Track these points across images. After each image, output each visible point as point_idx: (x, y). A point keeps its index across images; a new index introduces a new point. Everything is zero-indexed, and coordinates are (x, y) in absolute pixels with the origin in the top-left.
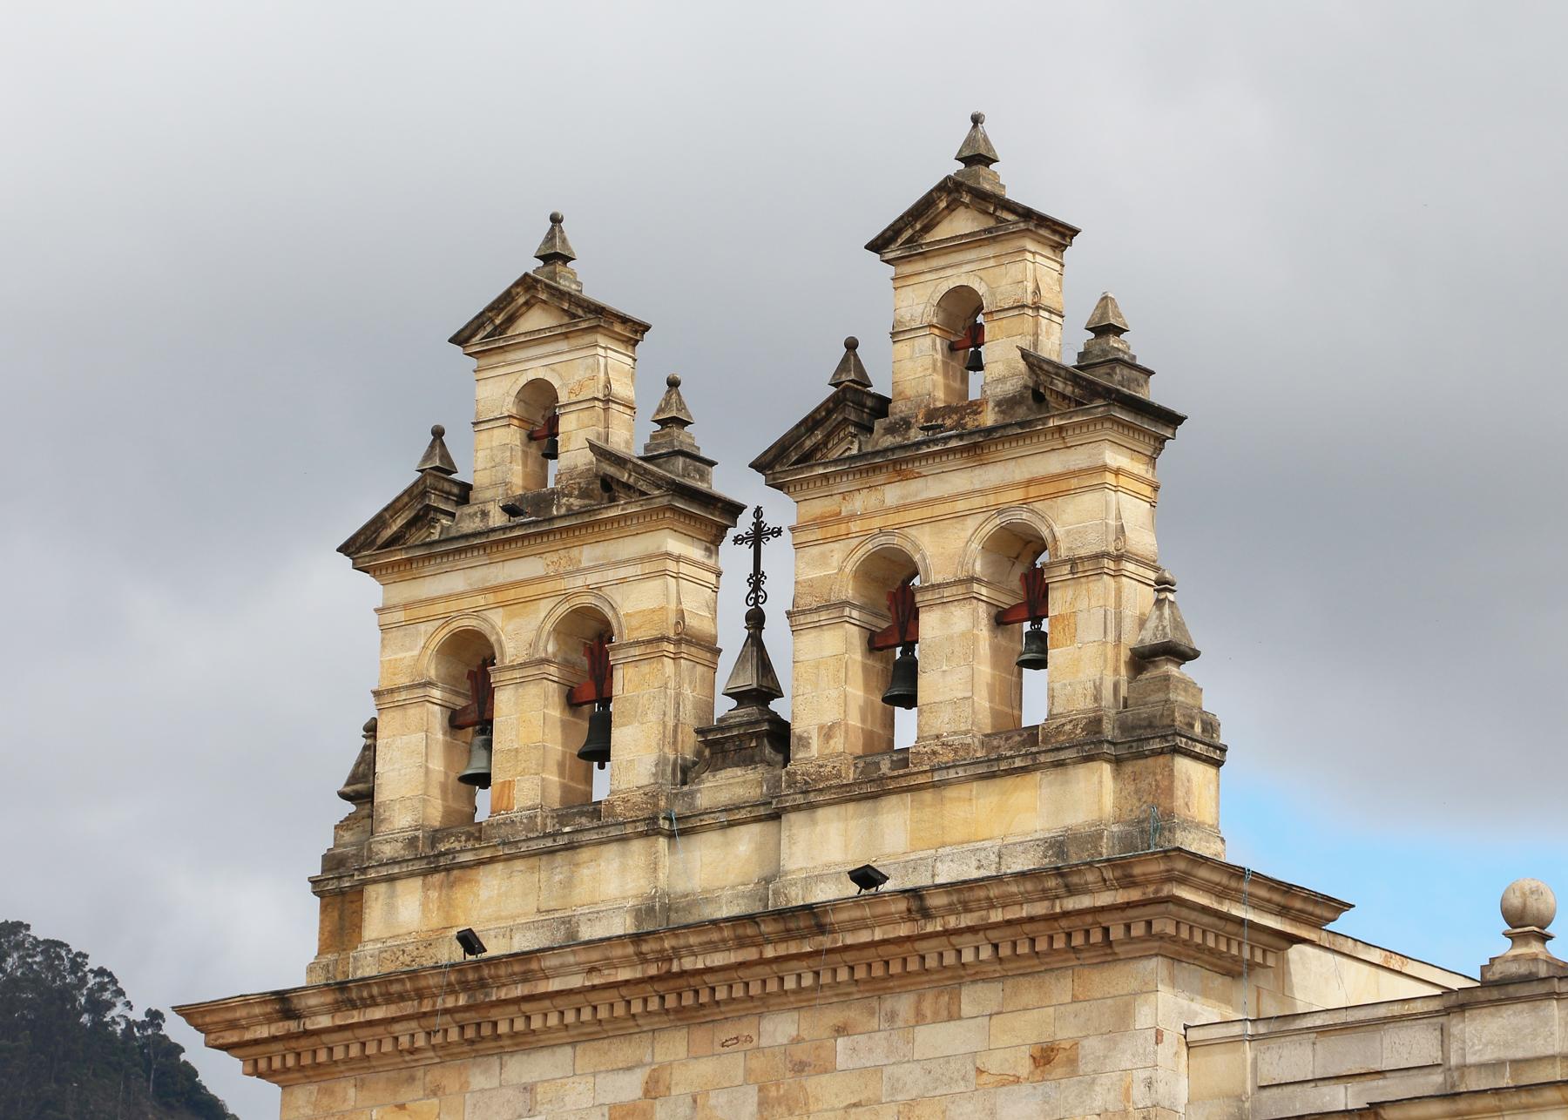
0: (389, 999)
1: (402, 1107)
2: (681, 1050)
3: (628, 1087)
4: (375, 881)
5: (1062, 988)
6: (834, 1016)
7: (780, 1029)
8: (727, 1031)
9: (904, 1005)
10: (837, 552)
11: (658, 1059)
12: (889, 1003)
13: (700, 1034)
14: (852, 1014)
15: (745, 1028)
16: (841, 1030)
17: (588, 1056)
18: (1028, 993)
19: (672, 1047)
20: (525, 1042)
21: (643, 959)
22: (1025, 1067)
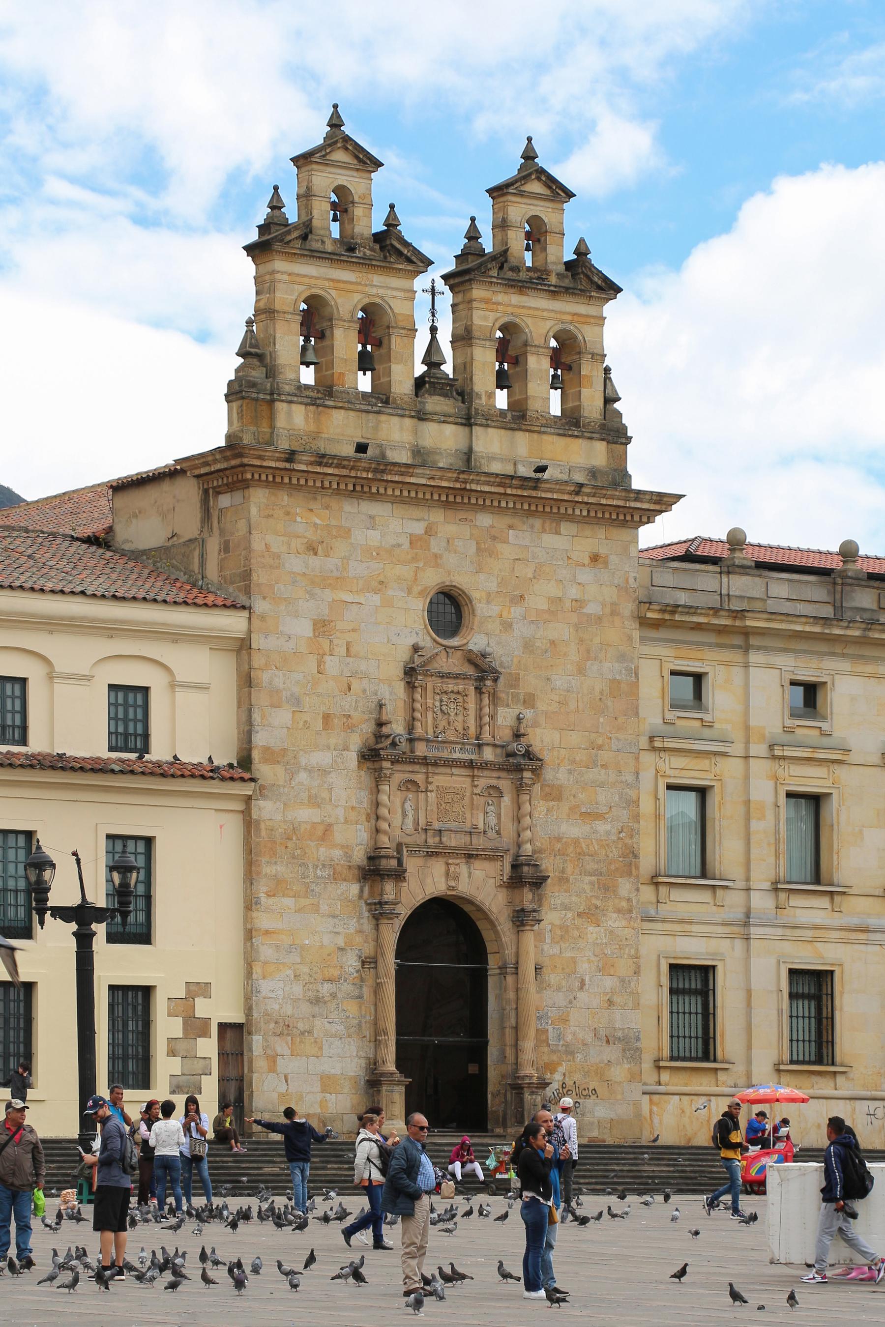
0: (338, 466)
1: (311, 510)
2: (442, 519)
3: (418, 528)
4: (282, 401)
5: (601, 532)
6: (507, 520)
7: (485, 520)
8: (462, 515)
9: (537, 523)
11: (432, 519)
12: (531, 521)
13: (450, 513)
14: (516, 521)
15: (469, 515)
16: (511, 527)
17: (399, 510)
18: (588, 531)
19: (437, 516)
20: (376, 497)
21: (457, 480)
22: (587, 561)
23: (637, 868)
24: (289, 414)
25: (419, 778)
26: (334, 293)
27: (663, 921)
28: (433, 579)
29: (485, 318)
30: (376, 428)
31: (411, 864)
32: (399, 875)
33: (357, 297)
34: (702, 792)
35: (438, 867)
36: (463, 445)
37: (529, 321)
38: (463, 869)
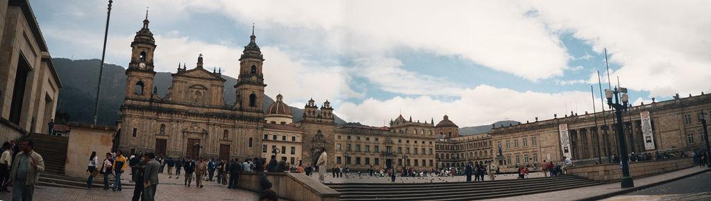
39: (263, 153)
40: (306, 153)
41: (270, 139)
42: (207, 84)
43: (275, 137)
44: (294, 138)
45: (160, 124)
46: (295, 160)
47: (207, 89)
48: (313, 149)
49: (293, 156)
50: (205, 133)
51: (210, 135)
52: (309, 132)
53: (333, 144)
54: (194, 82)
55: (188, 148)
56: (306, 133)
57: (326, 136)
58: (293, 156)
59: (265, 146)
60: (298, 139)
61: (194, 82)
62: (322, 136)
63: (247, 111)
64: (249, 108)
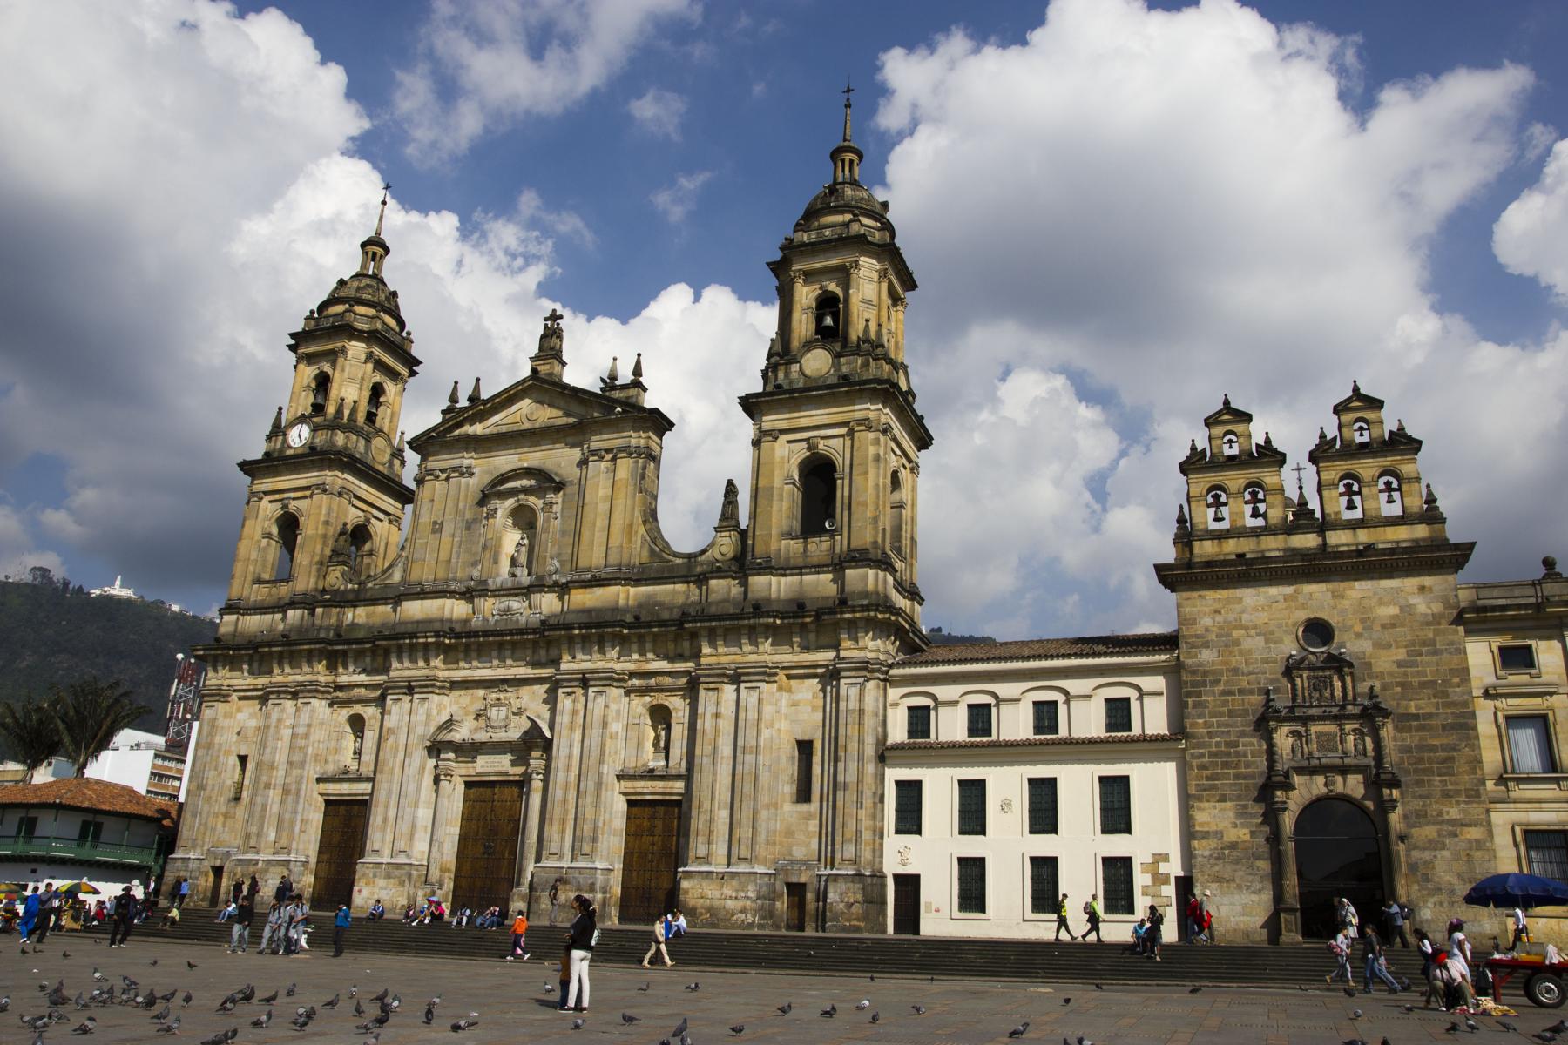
10: (1333, 473)
22: (1416, 591)
23: (1482, 769)
24: (1201, 546)
25: (1301, 729)
26: (1226, 482)
27: (1515, 802)
28: (1303, 615)
29: (1329, 475)
30: (1258, 543)
31: (1297, 780)
32: (1288, 787)
33: (1241, 481)
34: (1544, 717)
35: (1320, 780)
36: (1320, 540)
37: (1360, 471)
38: (1339, 779)
39: (894, 843)
40: (1215, 816)
41: (945, 737)
42: (561, 459)
43: (980, 718)
44: (1118, 712)
45: (345, 713)
46: (1140, 879)
47: (559, 486)
48: (1270, 788)
49: (1117, 845)
50: (535, 742)
51: (560, 749)
52: (1228, 644)
53: (1465, 725)
54: (506, 461)
55: (464, 839)
56: (1207, 656)
57: (1385, 662)
58: (1117, 845)
59: (910, 794)
60: (1153, 717)
61: (506, 461)
62: (1338, 664)
63: (783, 570)
64: (795, 546)
